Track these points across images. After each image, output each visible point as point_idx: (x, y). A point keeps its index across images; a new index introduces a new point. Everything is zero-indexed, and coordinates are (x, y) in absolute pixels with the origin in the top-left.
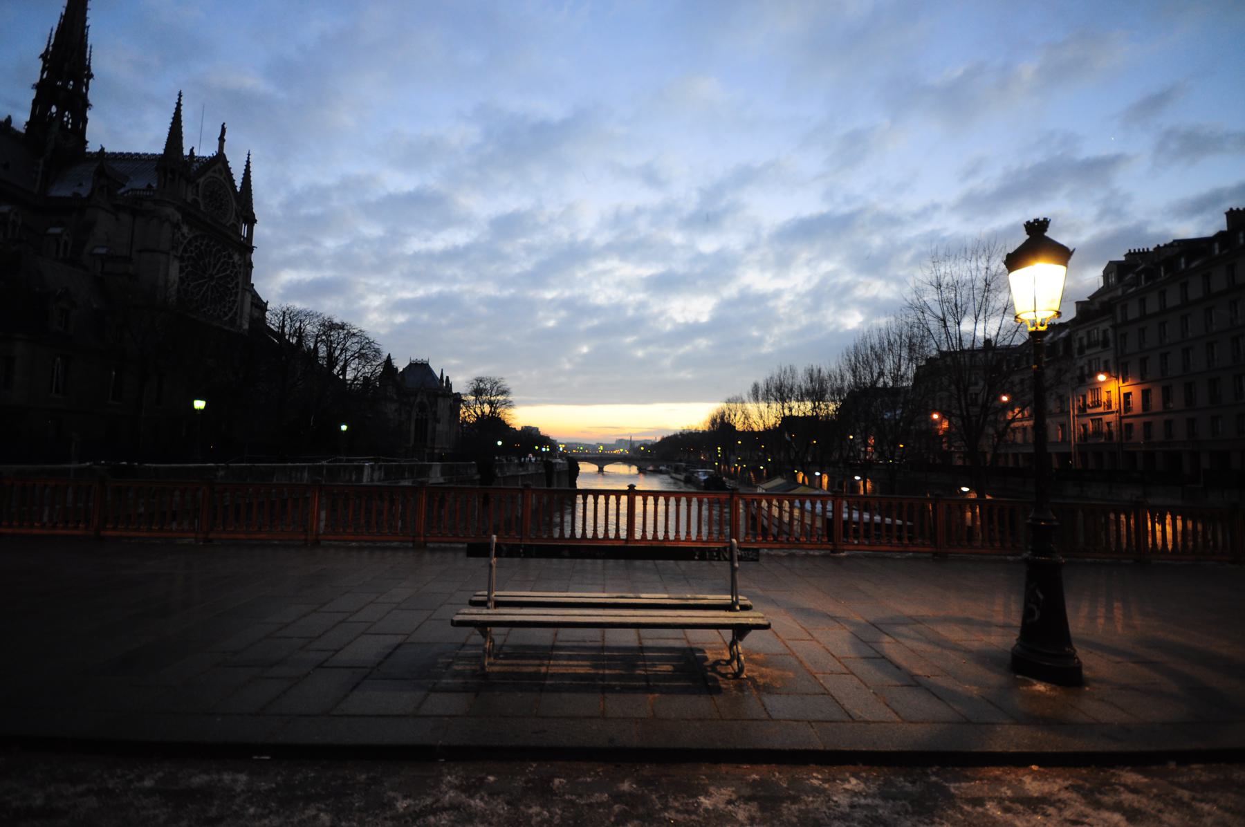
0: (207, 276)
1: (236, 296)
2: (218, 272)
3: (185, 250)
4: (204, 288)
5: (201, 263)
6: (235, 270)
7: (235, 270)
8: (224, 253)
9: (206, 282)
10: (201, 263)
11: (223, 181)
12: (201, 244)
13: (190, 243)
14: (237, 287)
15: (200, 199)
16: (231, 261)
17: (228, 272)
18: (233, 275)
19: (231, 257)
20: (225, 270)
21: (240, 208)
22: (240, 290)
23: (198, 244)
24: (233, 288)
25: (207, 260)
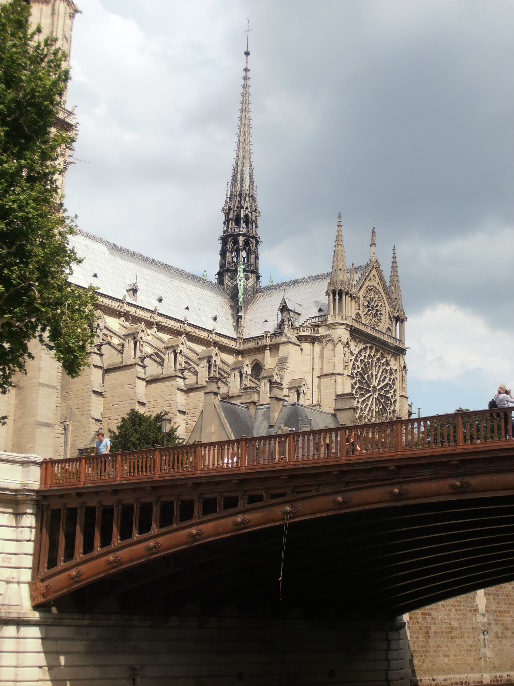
0: (371, 389)
1: (395, 406)
2: (378, 385)
3: (354, 368)
4: (370, 403)
5: (366, 377)
6: (392, 377)
7: (392, 377)
8: (382, 361)
9: (371, 395)
10: (366, 377)
11: (377, 286)
12: (365, 356)
13: (356, 360)
14: (395, 395)
15: (361, 312)
16: (389, 368)
17: (387, 381)
18: (391, 382)
19: (388, 364)
20: (383, 380)
21: (392, 310)
22: (397, 398)
23: (362, 358)
24: (392, 396)
25: (370, 372)
